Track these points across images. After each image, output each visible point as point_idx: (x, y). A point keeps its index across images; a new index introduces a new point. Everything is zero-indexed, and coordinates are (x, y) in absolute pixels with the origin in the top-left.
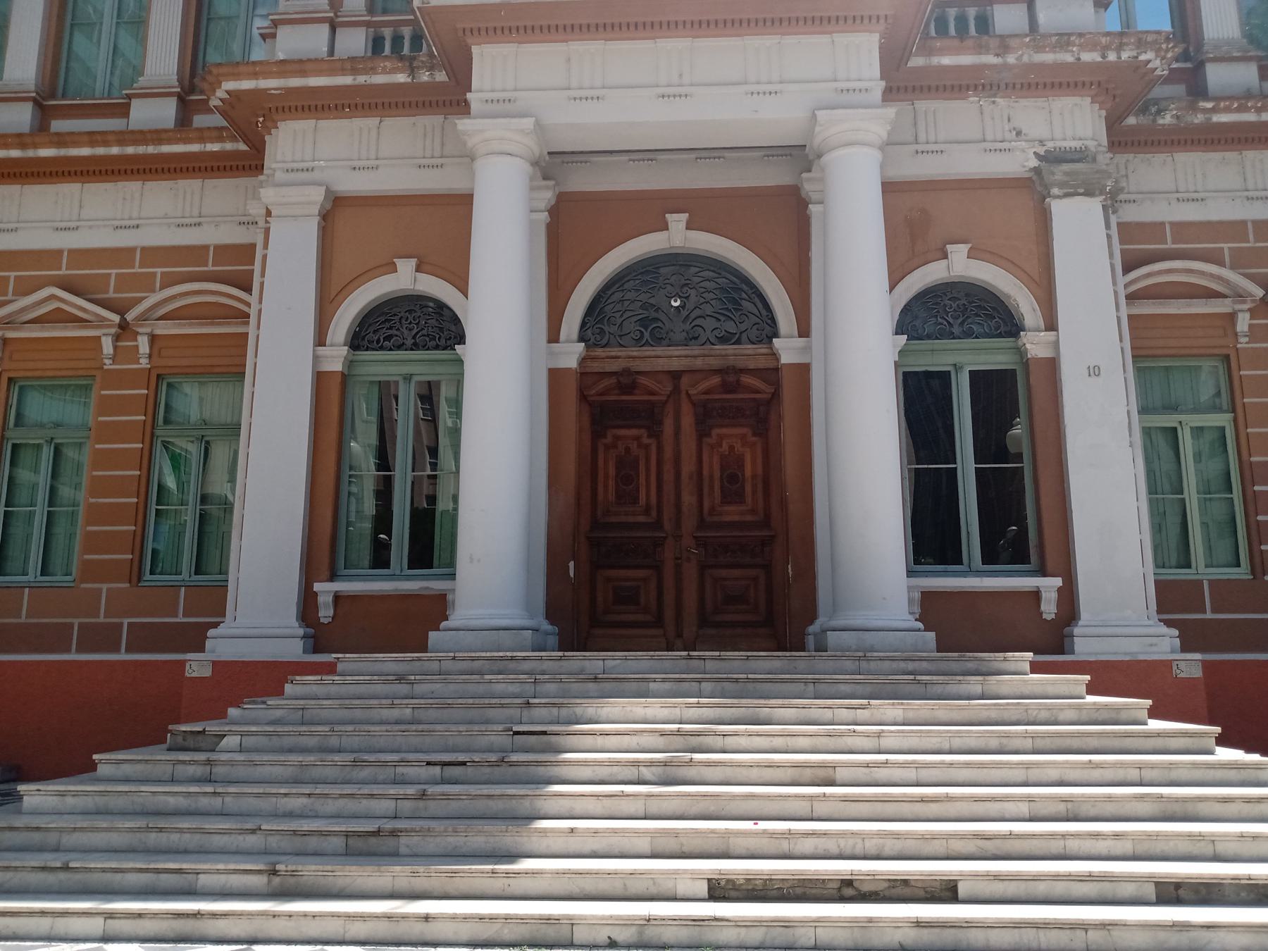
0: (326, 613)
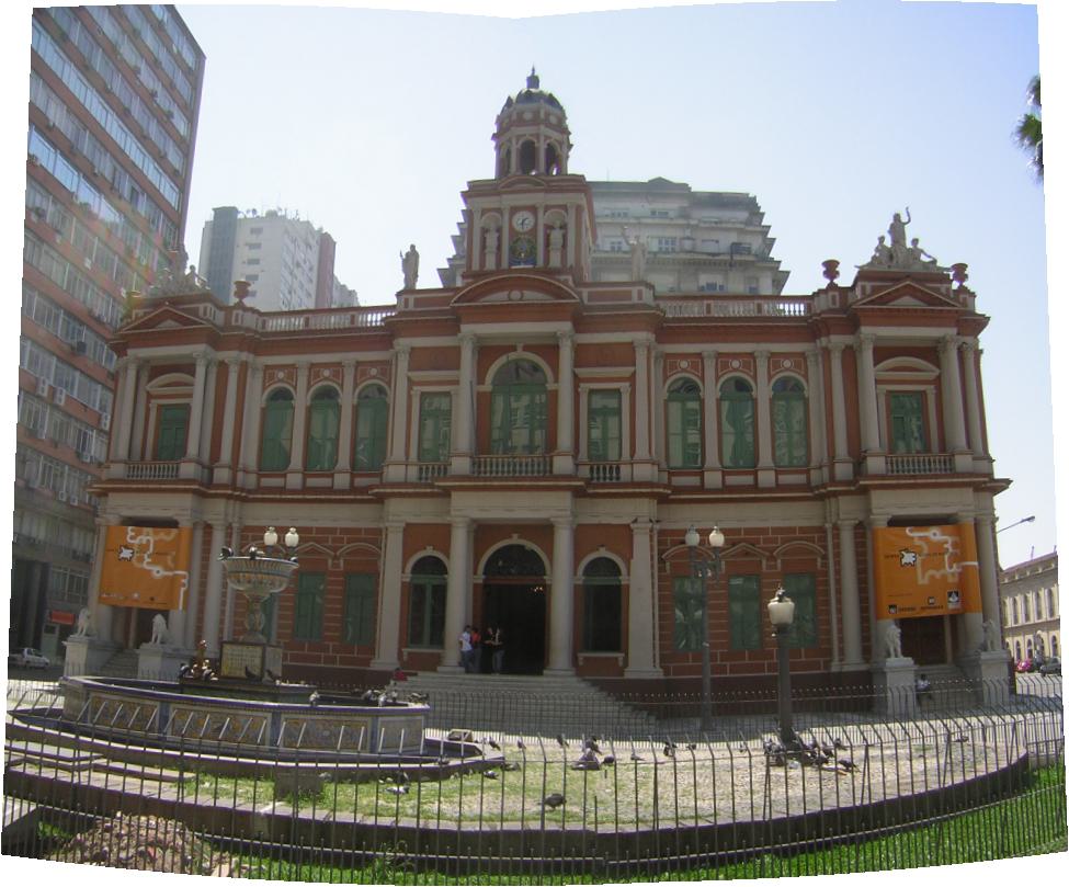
0: (405, 658)
